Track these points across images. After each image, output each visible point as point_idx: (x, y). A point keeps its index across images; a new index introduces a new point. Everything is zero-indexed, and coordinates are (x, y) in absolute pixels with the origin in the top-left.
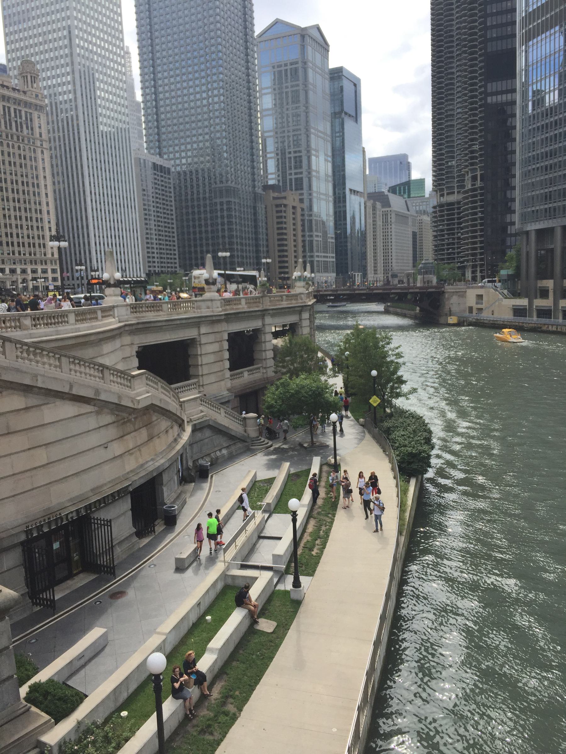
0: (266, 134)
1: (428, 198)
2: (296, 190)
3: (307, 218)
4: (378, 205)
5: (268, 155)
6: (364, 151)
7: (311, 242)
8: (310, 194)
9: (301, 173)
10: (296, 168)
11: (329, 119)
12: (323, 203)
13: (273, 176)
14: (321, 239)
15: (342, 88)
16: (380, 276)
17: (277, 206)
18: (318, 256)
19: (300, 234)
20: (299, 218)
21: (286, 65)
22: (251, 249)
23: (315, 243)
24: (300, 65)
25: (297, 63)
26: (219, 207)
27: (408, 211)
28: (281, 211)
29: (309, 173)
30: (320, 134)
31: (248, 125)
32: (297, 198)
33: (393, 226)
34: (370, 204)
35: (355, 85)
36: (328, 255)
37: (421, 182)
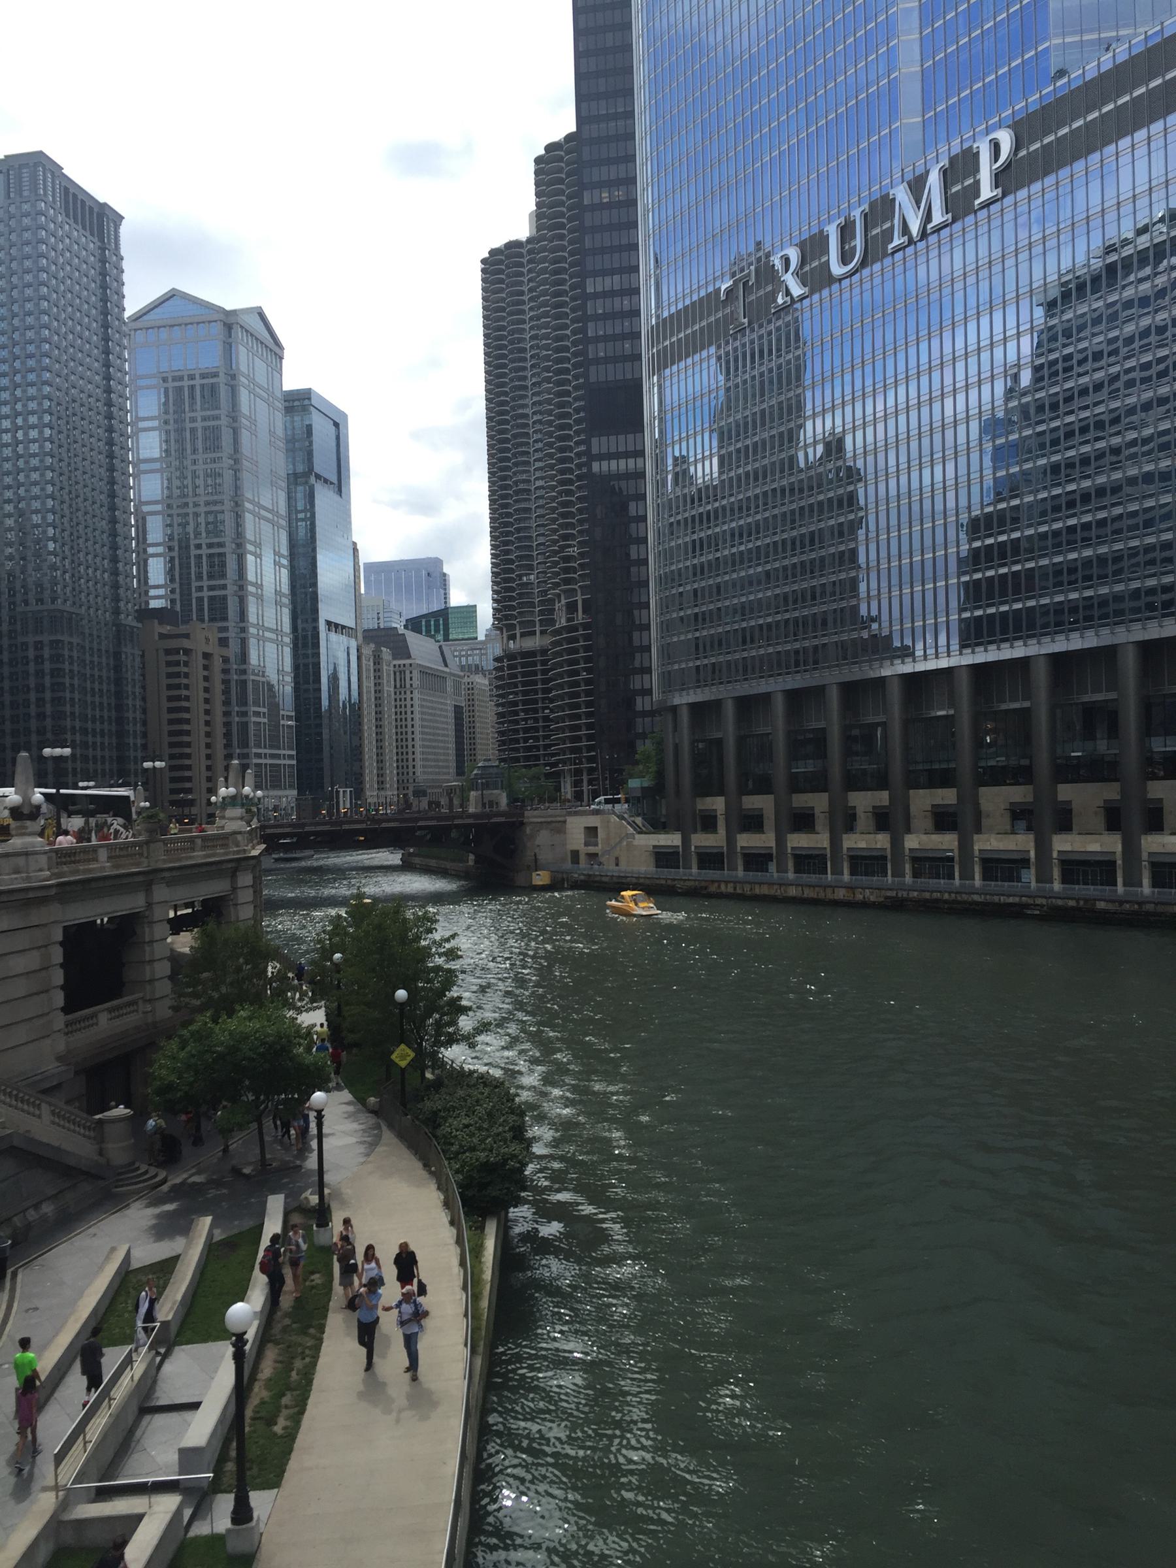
0: (145, 509)
1: (482, 642)
2: (211, 620)
3: (235, 677)
4: (386, 653)
5: (151, 550)
6: (355, 550)
7: (244, 726)
8: (243, 630)
9: (224, 587)
10: (211, 577)
11: (284, 485)
12: (271, 649)
13: (161, 592)
14: (266, 720)
15: (309, 429)
16: (391, 793)
17: (168, 652)
18: (258, 756)
19: (219, 709)
20: (218, 677)
21: (192, 377)
23: (252, 727)
24: (222, 379)
25: (216, 375)
26: (31, 653)
27: (446, 665)
28: (178, 663)
29: (241, 588)
30: (263, 513)
31: (106, 489)
32: (214, 636)
33: (416, 695)
34: (368, 651)
35: (336, 425)
36: (282, 752)
37: (469, 612)
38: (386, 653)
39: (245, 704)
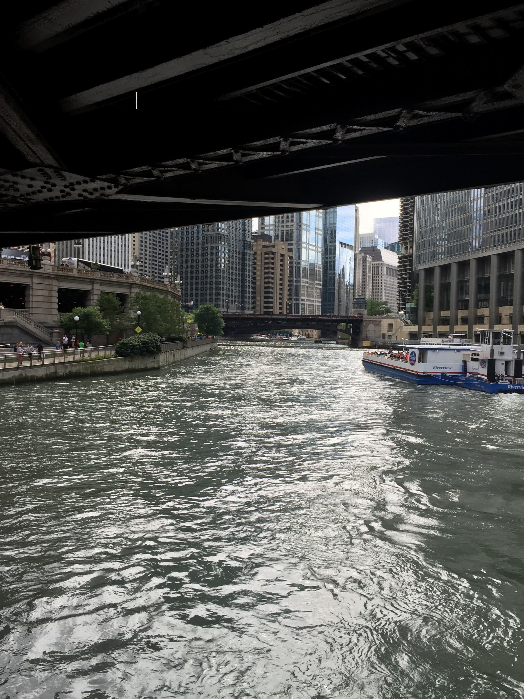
4: (369, 258)
7: (298, 287)
17: (266, 253)
18: (302, 300)
22: (237, 288)
29: (300, 226)
33: (384, 278)
34: (359, 257)
36: (315, 299)
38: (369, 258)
39: (299, 277)
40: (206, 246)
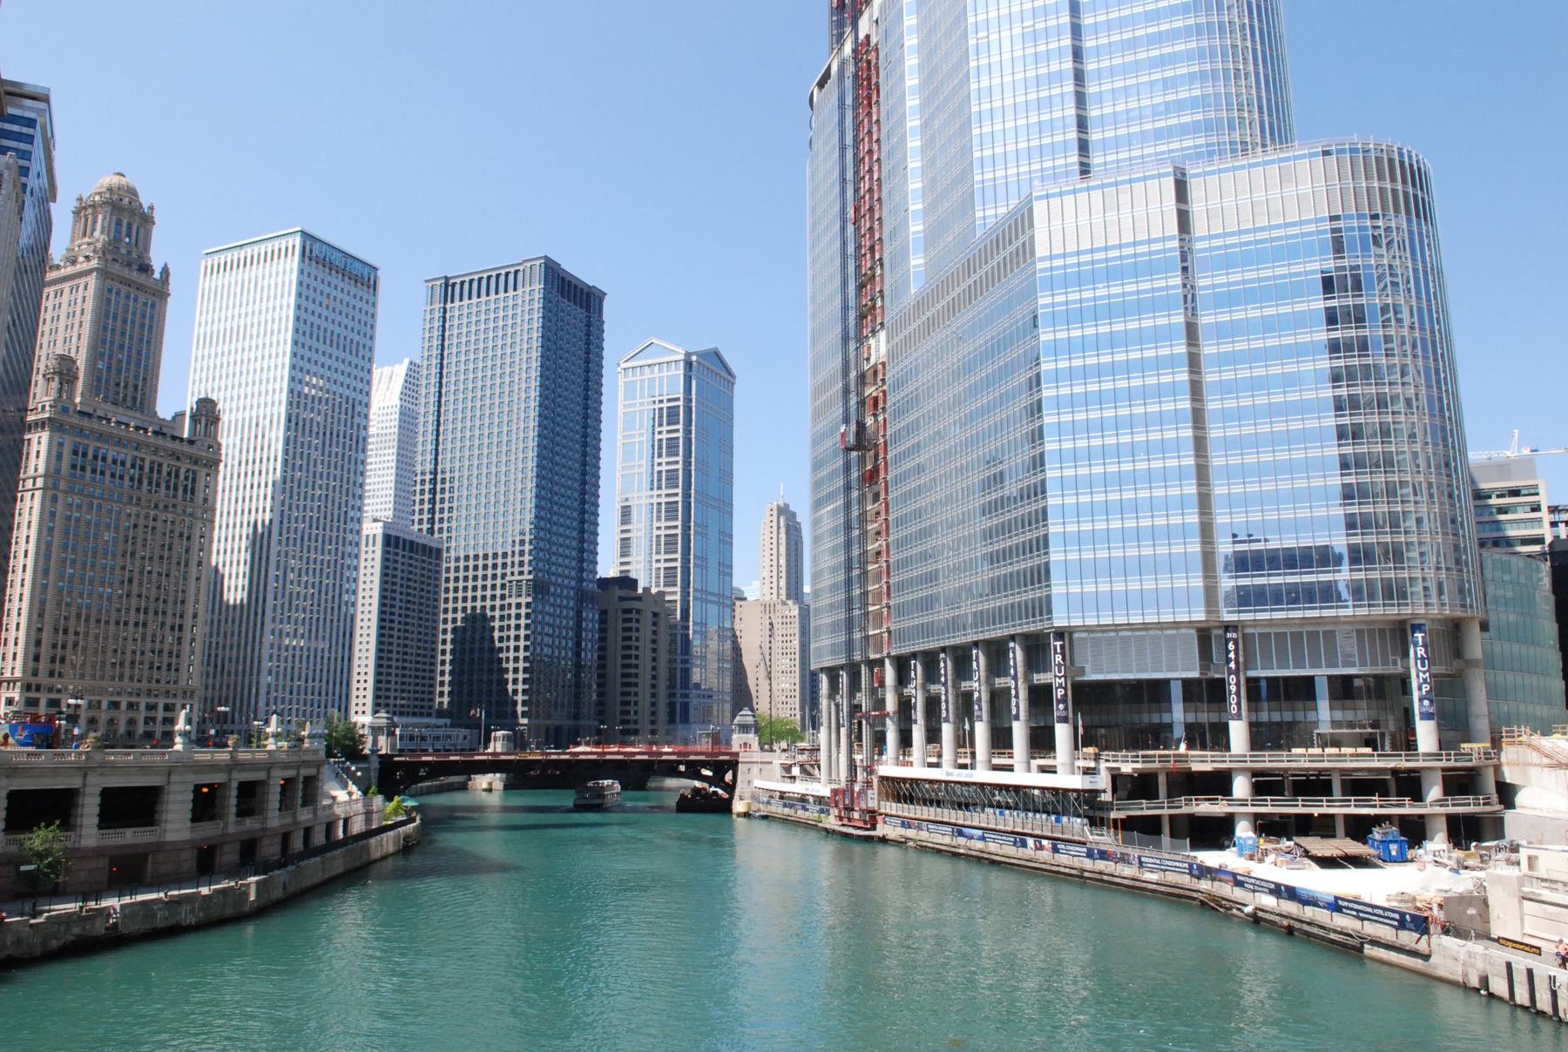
24: (681, 403)
40: (508, 601)
